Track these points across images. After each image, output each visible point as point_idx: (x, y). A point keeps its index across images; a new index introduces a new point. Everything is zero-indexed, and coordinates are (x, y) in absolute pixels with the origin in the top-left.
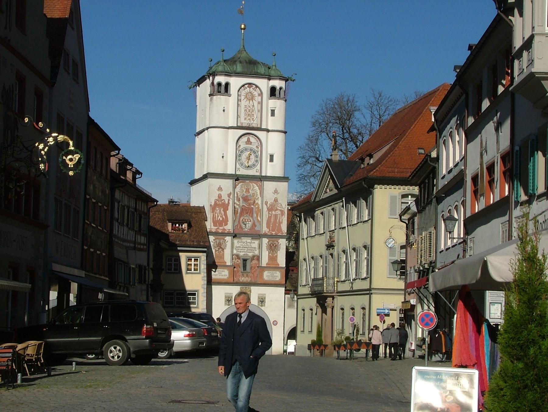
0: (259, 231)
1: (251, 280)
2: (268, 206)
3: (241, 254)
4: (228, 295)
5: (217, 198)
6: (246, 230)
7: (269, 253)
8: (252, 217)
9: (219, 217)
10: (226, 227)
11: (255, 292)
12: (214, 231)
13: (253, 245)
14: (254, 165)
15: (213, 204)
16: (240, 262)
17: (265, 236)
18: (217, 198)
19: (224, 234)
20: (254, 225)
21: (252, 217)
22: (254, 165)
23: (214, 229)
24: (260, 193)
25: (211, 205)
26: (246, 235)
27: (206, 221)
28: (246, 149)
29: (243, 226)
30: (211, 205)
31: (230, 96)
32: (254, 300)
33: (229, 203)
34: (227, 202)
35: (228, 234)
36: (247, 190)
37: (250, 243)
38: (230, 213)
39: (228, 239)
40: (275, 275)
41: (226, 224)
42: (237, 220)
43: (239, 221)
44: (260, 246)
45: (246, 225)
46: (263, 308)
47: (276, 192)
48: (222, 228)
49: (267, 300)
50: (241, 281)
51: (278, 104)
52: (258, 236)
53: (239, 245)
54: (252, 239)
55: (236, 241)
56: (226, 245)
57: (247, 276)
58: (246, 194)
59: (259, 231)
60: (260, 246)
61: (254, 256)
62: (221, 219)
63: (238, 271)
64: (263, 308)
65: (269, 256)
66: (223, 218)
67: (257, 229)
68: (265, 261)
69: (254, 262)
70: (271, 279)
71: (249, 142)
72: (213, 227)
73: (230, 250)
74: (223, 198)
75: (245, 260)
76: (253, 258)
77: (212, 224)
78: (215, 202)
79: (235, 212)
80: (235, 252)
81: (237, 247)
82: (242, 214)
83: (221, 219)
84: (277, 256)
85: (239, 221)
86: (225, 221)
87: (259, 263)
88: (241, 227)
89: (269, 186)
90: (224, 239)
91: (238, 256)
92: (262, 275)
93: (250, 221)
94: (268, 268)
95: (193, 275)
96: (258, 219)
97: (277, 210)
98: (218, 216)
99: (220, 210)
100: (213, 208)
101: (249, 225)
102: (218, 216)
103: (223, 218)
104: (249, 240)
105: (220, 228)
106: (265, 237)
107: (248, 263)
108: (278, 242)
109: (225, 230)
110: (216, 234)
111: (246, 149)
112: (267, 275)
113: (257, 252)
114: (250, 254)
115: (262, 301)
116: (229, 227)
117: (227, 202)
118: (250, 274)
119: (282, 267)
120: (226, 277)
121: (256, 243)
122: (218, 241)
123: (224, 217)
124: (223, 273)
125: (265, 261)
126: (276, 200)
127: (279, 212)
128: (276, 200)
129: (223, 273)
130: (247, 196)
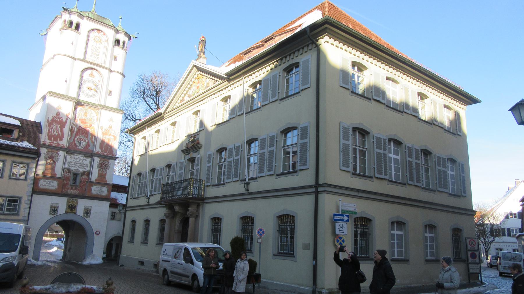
0: (92, 151)
1: (79, 193)
2: (103, 130)
3: (73, 169)
4: (54, 205)
5: (55, 115)
6: (80, 148)
7: (99, 171)
8: (87, 137)
9: (55, 133)
10: (60, 143)
11: (82, 204)
12: (47, 144)
13: (85, 162)
14: (94, 95)
15: (50, 119)
16: (71, 176)
17: (98, 155)
18: (55, 115)
19: (58, 148)
20: (88, 145)
21: (87, 137)
22: (94, 95)
23: (48, 142)
24: (97, 119)
25: (48, 120)
26: (80, 152)
27: (41, 133)
28: (89, 81)
29: (78, 144)
30: (48, 120)
31: (79, 34)
32: (80, 211)
33: (66, 121)
34: (64, 120)
35: (63, 149)
36: (86, 114)
37: (83, 160)
38: (66, 130)
39: (62, 153)
40: (103, 190)
41: (61, 140)
42: (73, 138)
43: (74, 140)
44: (91, 164)
45: (80, 143)
46: (87, 219)
47: (111, 120)
48: (56, 142)
49: (92, 212)
50: (69, 193)
51: (119, 51)
52: (91, 155)
53: (71, 161)
54: (85, 156)
55: (69, 157)
56: (58, 159)
57: (76, 189)
58: (84, 118)
59: (92, 151)
60: (91, 164)
61: (84, 172)
62: (57, 134)
63: (67, 184)
64: (87, 219)
65: (99, 173)
66: (59, 134)
67: (90, 148)
68: (94, 176)
69: (84, 177)
70: (98, 193)
71: (92, 75)
72: (47, 140)
73: (61, 164)
74: (61, 116)
75: (76, 175)
76: (83, 173)
77: (47, 137)
78: (53, 119)
79: (72, 131)
80: (67, 166)
81: (69, 162)
82: (77, 134)
83: (57, 134)
84: (106, 174)
85: (74, 140)
86: (61, 137)
87: (89, 179)
88: (75, 145)
89: (105, 113)
90: (57, 153)
91: (69, 171)
92: (90, 190)
93: (85, 141)
94: (96, 183)
95: (18, 181)
96: (92, 141)
97: (110, 135)
98: (54, 131)
99: (57, 127)
100: (50, 123)
101: (84, 144)
102: (54, 131)
103: (59, 134)
104: (81, 157)
105: (55, 142)
106: (96, 156)
107: (79, 178)
108: (108, 161)
109: (59, 145)
110: (49, 147)
111: (89, 81)
112: (95, 190)
113: (87, 169)
114: (81, 170)
115: (87, 212)
116: (64, 142)
117: (64, 120)
118: (79, 188)
119: (109, 184)
120: (54, 188)
121: (88, 161)
122: (50, 154)
123: (60, 133)
124: (52, 184)
125: (94, 176)
126: (110, 127)
127: (112, 137)
128: (110, 127)
129: (52, 184)
130: (84, 119)
